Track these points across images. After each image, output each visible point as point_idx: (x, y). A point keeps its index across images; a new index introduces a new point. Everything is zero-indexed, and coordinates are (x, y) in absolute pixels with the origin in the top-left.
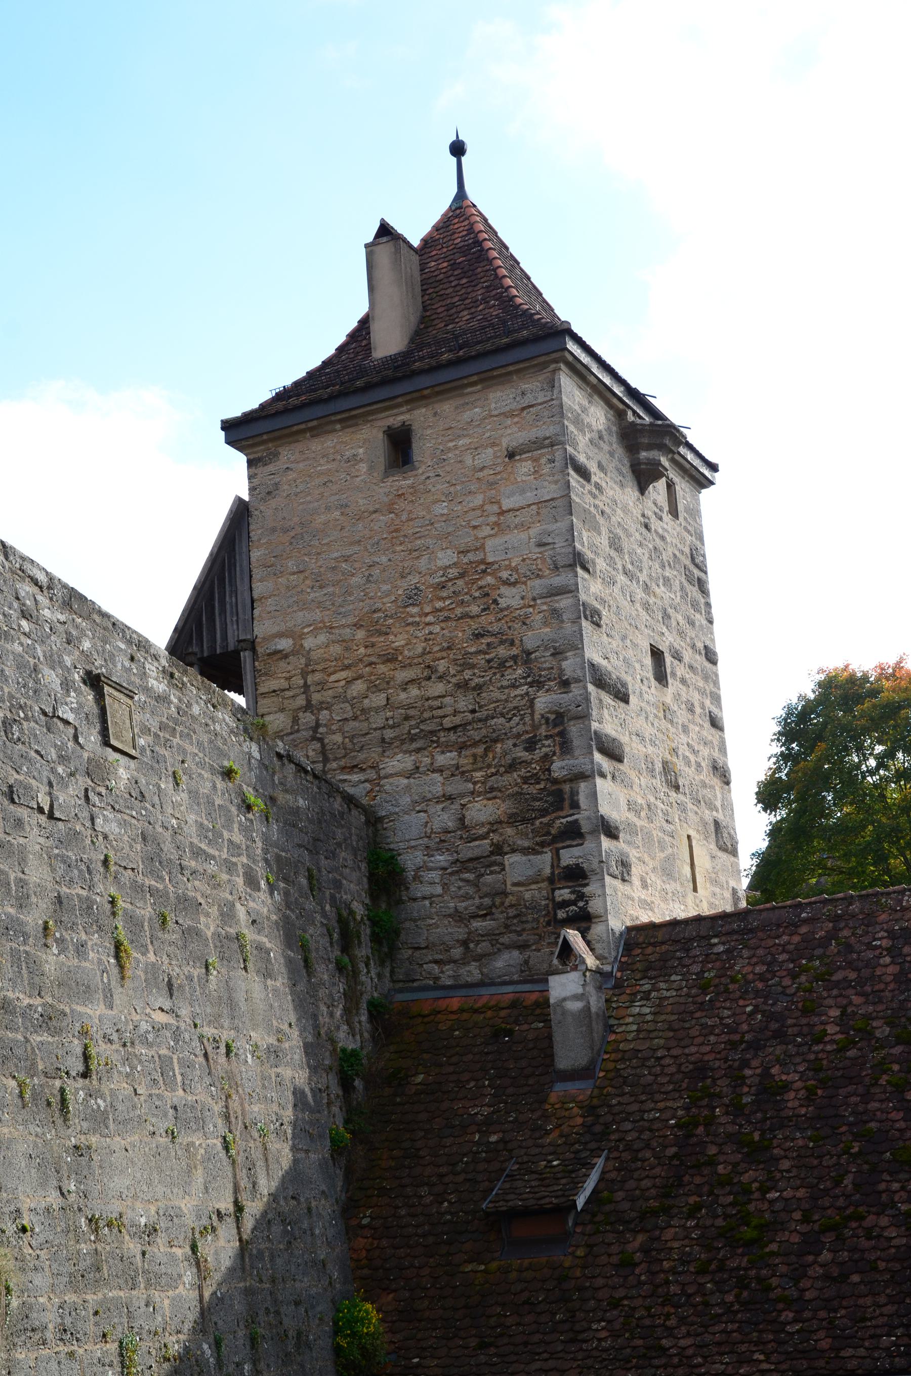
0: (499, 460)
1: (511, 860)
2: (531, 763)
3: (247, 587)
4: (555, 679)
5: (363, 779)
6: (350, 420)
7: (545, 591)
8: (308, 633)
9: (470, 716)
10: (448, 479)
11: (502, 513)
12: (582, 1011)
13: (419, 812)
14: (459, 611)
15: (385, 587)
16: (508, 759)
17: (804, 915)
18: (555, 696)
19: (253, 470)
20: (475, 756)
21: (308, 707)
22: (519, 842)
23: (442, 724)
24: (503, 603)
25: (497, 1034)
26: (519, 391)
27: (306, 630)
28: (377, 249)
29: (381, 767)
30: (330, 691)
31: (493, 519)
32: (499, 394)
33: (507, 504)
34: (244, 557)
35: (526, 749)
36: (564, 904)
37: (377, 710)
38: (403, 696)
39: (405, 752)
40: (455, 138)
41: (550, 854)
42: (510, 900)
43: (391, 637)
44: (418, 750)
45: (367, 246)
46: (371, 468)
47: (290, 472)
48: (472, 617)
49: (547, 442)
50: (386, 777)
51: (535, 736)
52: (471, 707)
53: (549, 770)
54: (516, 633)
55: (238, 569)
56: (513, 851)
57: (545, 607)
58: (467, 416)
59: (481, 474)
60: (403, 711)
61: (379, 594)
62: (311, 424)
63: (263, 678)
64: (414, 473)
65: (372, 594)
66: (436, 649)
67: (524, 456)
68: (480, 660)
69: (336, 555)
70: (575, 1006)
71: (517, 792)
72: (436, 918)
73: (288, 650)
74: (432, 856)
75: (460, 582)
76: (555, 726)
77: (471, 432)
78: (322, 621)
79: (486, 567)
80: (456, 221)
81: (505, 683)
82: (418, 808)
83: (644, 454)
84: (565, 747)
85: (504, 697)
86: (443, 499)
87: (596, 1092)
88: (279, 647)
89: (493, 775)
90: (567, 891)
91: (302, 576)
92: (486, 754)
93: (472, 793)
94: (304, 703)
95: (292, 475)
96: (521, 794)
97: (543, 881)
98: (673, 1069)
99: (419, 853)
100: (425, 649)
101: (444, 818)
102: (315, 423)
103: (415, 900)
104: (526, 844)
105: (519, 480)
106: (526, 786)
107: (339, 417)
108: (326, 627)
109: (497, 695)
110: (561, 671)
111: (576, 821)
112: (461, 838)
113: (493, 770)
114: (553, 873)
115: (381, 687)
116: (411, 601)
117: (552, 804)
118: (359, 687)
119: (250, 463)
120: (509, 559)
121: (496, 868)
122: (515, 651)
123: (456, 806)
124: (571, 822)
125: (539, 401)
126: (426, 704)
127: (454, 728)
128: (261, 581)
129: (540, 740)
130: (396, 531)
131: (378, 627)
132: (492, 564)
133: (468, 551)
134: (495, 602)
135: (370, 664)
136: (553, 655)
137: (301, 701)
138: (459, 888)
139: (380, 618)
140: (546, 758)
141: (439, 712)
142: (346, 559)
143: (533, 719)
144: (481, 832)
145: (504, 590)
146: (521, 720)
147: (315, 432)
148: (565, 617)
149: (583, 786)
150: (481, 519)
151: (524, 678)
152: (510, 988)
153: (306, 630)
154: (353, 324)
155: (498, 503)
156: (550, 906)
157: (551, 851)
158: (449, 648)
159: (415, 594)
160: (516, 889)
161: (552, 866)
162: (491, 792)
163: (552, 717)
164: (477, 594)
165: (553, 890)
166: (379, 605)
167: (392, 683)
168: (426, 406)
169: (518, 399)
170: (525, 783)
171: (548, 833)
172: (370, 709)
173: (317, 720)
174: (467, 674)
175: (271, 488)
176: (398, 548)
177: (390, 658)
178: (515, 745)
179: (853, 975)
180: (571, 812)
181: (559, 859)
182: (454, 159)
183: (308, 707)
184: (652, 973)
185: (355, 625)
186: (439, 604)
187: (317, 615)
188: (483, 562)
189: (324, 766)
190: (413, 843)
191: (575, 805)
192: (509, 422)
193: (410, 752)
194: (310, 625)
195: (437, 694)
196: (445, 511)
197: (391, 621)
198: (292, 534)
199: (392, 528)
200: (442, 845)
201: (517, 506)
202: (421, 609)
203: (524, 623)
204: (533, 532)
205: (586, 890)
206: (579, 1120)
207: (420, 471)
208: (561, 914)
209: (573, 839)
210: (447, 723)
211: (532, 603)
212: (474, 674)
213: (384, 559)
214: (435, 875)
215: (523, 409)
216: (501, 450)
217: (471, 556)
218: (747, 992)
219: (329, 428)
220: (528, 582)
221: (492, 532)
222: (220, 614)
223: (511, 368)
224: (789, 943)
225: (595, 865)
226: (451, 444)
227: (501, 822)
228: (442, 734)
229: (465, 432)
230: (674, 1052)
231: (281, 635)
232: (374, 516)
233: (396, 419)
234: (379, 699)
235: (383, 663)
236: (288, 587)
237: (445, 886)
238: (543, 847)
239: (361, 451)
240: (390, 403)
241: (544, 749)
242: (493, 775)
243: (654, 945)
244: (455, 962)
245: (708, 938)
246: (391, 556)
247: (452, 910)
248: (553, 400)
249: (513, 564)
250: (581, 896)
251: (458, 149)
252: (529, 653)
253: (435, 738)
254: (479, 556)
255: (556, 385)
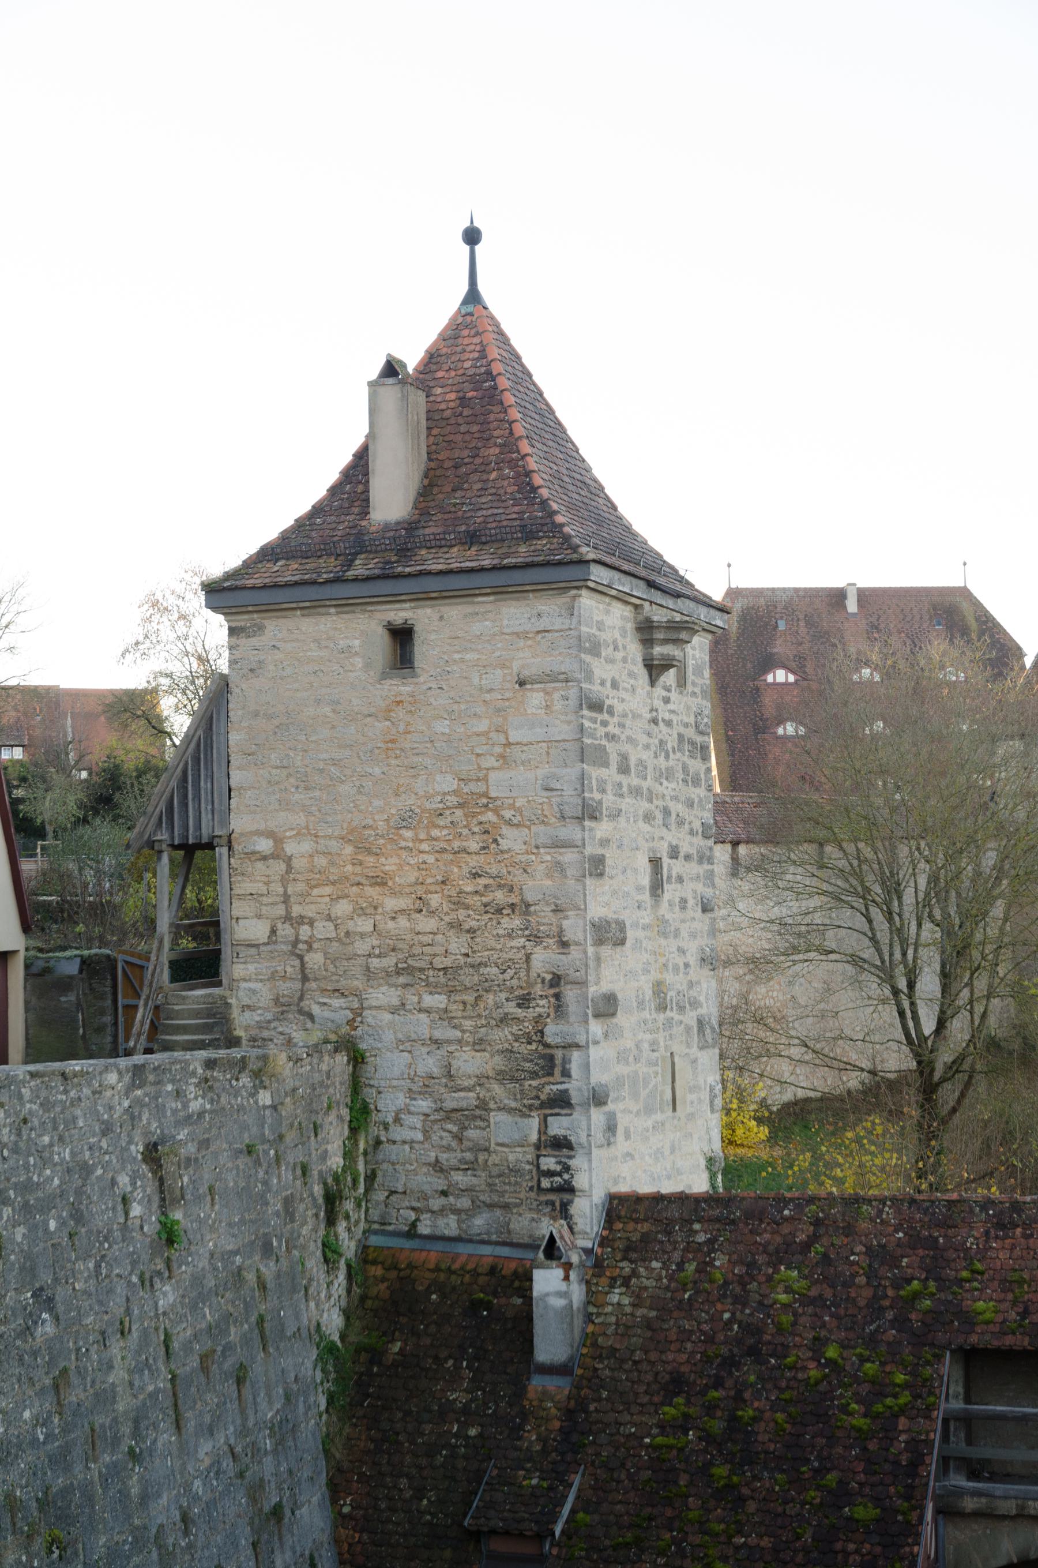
0: (508, 685)
1: (497, 1119)
2: (523, 1021)
3: (224, 774)
4: (554, 937)
5: (344, 1006)
6: (345, 605)
7: (549, 841)
8: (290, 837)
9: (462, 960)
10: (452, 694)
11: (509, 744)
12: (565, 1308)
13: (403, 1051)
14: (456, 844)
15: (377, 803)
16: (498, 1014)
17: (786, 1212)
18: (553, 956)
19: (234, 640)
20: (464, 1003)
21: (288, 918)
22: (506, 1101)
23: (431, 963)
24: (504, 844)
25: (476, 1306)
26: (535, 612)
27: (288, 834)
28: (382, 390)
29: (364, 996)
30: (312, 906)
31: (498, 750)
32: (512, 610)
33: (514, 736)
34: (222, 738)
35: (519, 1006)
36: (550, 1174)
37: (362, 935)
38: (391, 925)
39: (391, 985)
40: (468, 224)
41: (537, 1119)
42: (494, 1159)
43: (383, 860)
44: (405, 986)
45: (372, 384)
46: (367, 666)
47: (276, 651)
48: (468, 853)
49: (562, 677)
50: (370, 1008)
51: (529, 994)
52: (464, 951)
53: (542, 1032)
54: (515, 879)
55: (215, 751)
56: (499, 1109)
57: (549, 858)
58: (477, 628)
59: (488, 697)
60: (391, 942)
61: (370, 809)
62: (302, 605)
63: (240, 878)
64: (415, 680)
65: (363, 807)
66: (429, 880)
67: (536, 686)
68: (475, 901)
69: (324, 756)
70: (559, 1303)
71: (507, 1049)
72: (415, 1164)
73: (269, 852)
74: (415, 1099)
75: (459, 813)
76: (551, 986)
77: (480, 647)
78: (307, 828)
79: (490, 803)
80: (465, 332)
81: (501, 932)
82: (401, 1047)
83: (658, 650)
84: (559, 1008)
85: (499, 947)
86: (446, 716)
87: (574, 1391)
88: (258, 848)
89: (483, 1026)
90: (553, 1160)
91: (285, 772)
92: (475, 1004)
93: (460, 1041)
94: (283, 913)
95: (279, 655)
96: (511, 1052)
97: (529, 1145)
98: (649, 1377)
99: (401, 1095)
100: (418, 879)
101: (429, 1063)
102: (307, 604)
103: (394, 1142)
104: (513, 1104)
105: (529, 712)
106: (516, 1044)
107: (334, 603)
108: (311, 835)
109: (492, 943)
110: (561, 932)
111: (566, 1091)
112: (446, 1086)
113: (484, 1022)
114: (539, 1139)
115: (368, 911)
116: (404, 824)
117: (542, 1068)
118: (343, 908)
119: (232, 631)
120: (514, 798)
121: (479, 1123)
122: (514, 899)
123: (442, 1052)
124: (561, 1091)
125: (556, 628)
126: (416, 938)
127: (445, 969)
128: (238, 768)
129: (534, 999)
130: (393, 741)
131: (368, 846)
132: (495, 799)
133: (470, 780)
134: (495, 841)
135: (359, 884)
136: (553, 911)
137: (280, 910)
138: (441, 1138)
139: (370, 836)
140: (538, 1019)
141: (428, 950)
142: (335, 762)
143: (528, 976)
144: (466, 1084)
145: (505, 830)
146: (515, 973)
147: (305, 612)
148: (568, 873)
149: (576, 1055)
150: (485, 747)
151: (521, 929)
152: (486, 1250)
153: (288, 834)
154: (346, 458)
155: (506, 733)
156: (534, 1172)
157: (539, 1115)
158: (443, 882)
159: (410, 817)
160: (499, 1148)
161: (539, 1132)
162: (479, 1045)
163: (548, 977)
164: (476, 829)
165: (538, 1157)
166: (370, 822)
167: (380, 910)
168: (432, 606)
169: (533, 620)
170: (516, 1041)
171: (537, 1097)
172: (355, 933)
173: (297, 935)
174: (462, 914)
175: (254, 666)
176: (393, 762)
177: (380, 881)
178: (507, 1000)
179: (828, 1293)
180: (563, 1079)
181: (546, 1127)
182: (467, 248)
183: (288, 918)
184: (634, 1256)
185: (343, 839)
186: (435, 833)
187: (301, 819)
188: (485, 795)
189: (303, 985)
190: (395, 1083)
191: (566, 1074)
192: (521, 643)
193: (396, 986)
194: (292, 829)
195: (428, 930)
196: (447, 731)
197: (382, 841)
198: (276, 722)
199: (388, 737)
200: (426, 1091)
201: (525, 741)
202: (416, 835)
203: (525, 871)
204: (540, 773)
205: (572, 1163)
206: (557, 1424)
207: (422, 679)
208: (546, 1183)
209: (562, 1107)
210: (439, 962)
211: (535, 851)
212: (469, 916)
213: (377, 771)
214: (417, 1121)
215: (538, 632)
216: (511, 674)
217: (472, 787)
218: (725, 1296)
219: (323, 610)
220: (533, 827)
221: (496, 764)
222: (193, 799)
223: (528, 588)
224: (768, 1243)
225: (583, 1139)
226: (457, 656)
227: (488, 1078)
228: (431, 973)
229: (473, 646)
230: (653, 1356)
231: (259, 833)
232: (369, 719)
233: (399, 614)
234: (365, 925)
235: (371, 886)
236: (270, 782)
237: (425, 1132)
238: (531, 1110)
239: (357, 643)
240: (394, 599)
241: (538, 1009)
242: (483, 1026)
243: (637, 1221)
244: (433, 1212)
245: (691, 1222)
246: (385, 769)
247: (433, 1159)
248: (570, 629)
249: (517, 805)
250: (567, 1168)
251: (472, 237)
252: (528, 906)
253: (423, 977)
254: (481, 787)
255: (576, 613)
